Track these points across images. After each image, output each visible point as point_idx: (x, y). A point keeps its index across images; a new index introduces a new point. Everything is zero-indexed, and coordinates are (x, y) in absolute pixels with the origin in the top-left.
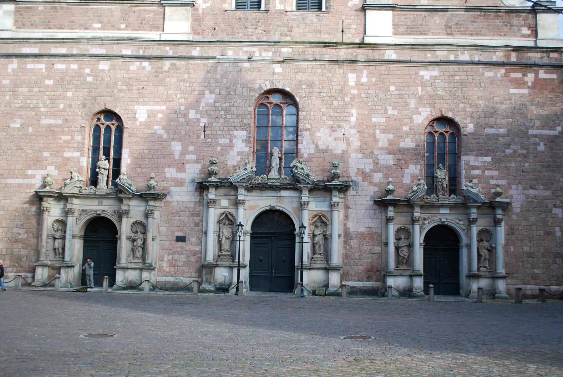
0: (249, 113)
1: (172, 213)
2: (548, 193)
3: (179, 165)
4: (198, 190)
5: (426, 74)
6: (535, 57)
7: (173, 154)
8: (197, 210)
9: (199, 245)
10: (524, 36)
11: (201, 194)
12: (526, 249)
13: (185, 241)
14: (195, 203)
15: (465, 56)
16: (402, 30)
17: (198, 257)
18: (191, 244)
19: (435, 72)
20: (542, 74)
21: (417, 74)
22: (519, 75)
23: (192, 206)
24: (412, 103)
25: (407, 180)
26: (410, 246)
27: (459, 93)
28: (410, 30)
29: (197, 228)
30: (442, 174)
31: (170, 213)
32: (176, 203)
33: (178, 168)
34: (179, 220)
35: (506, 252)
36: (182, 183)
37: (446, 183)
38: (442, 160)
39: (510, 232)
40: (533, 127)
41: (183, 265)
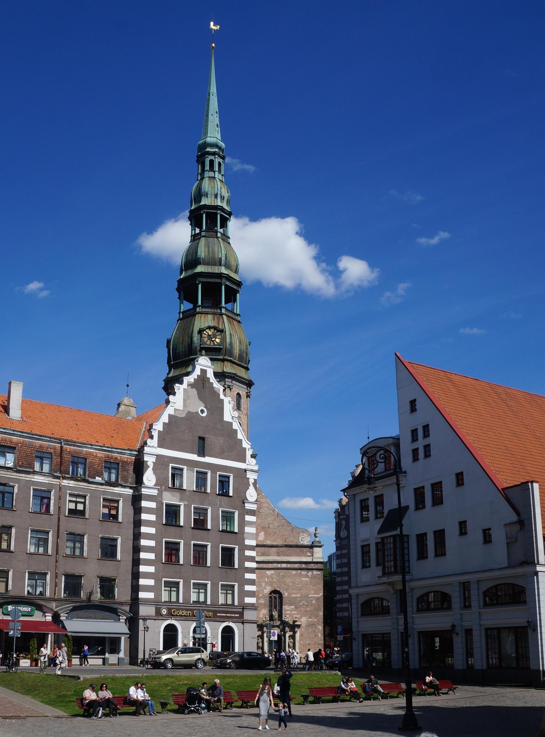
2: (316, 620)
5: (269, 573)
6: (312, 566)
10: (308, 556)
12: (307, 642)
15: (284, 566)
16: (259, 554)
19: (272, 572)
20: (315, 572)
21: (265, 573)
22: (306, 573)
24: (263, 585)
25: (261, 616)
26: (263, 642)
27: (282, 580)
28: (263, 554)
30: (275, 614)
35: (300, 643)
37: (277, 616)
38: (275, 607)
39: (301, 635)
40: (310, 594)
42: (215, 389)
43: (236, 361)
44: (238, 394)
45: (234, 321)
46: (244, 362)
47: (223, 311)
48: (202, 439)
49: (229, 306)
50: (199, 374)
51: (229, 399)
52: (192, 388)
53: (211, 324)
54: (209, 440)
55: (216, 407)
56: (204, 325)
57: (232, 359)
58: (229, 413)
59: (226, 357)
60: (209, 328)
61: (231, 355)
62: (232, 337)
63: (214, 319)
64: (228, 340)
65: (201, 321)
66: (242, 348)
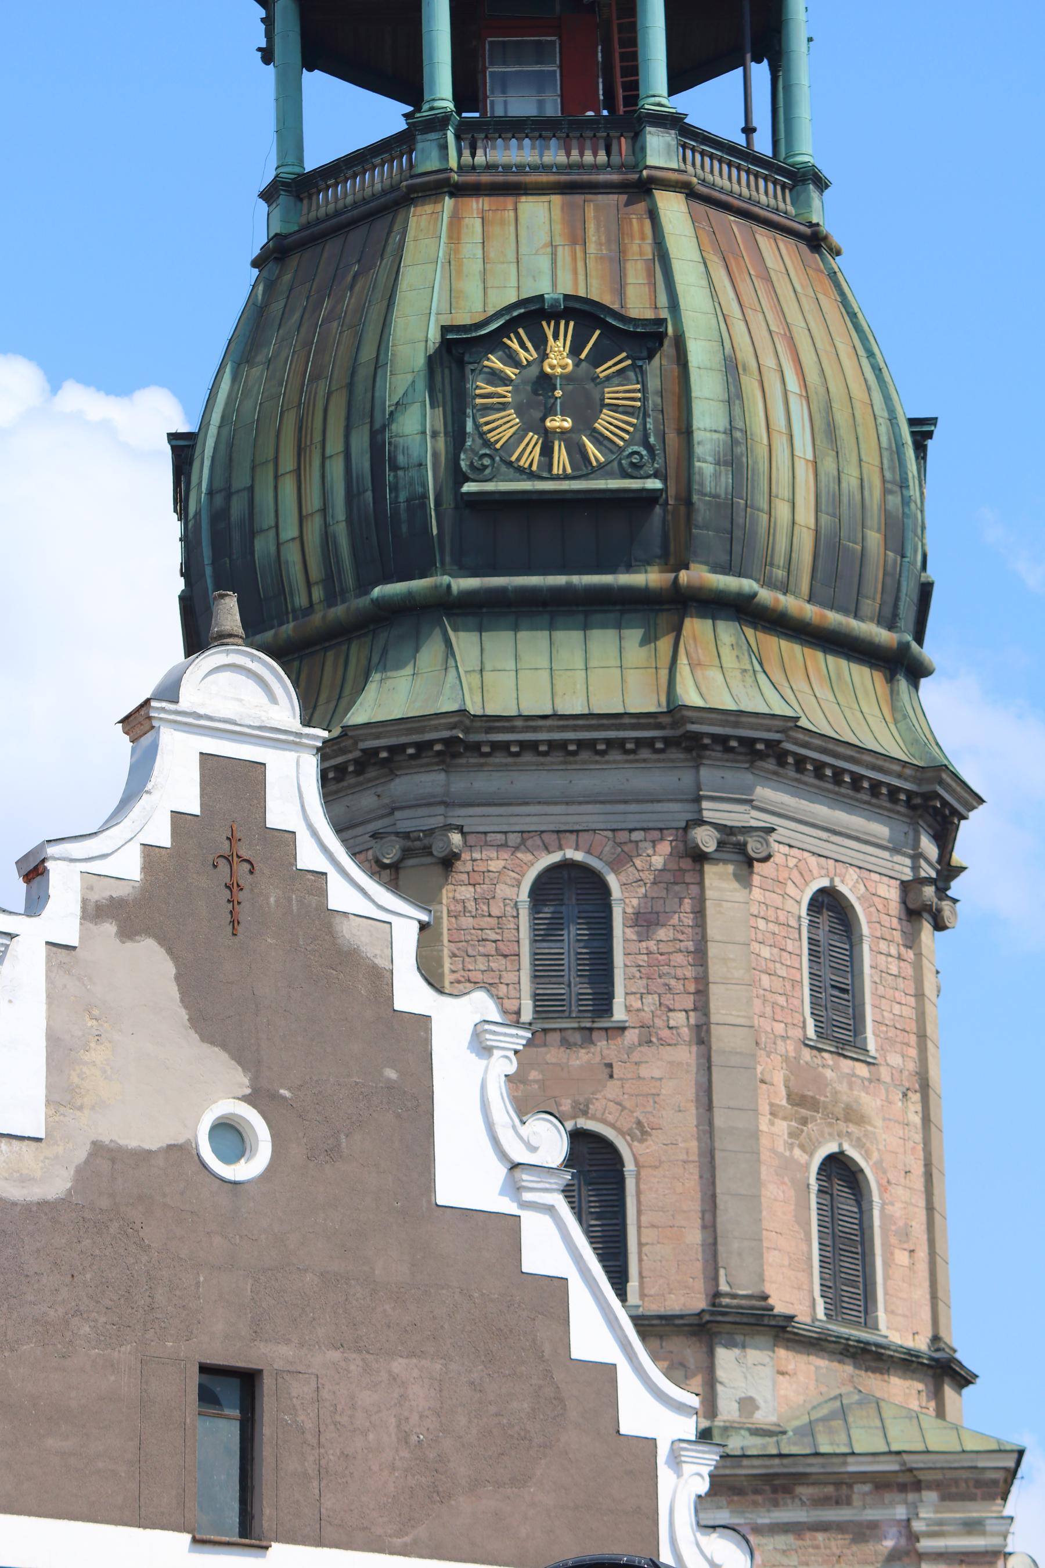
42: (350, 932)
43: (795, 605)
44: (829, 904)
45: (764, 239)
46: (870, 606)
47: (659, 150)
48: (233, 1388)
49: (717, 104)
50: (193, 806)
51: (480, 1005)
52: (127, 933)
53: (550, 278)
54: (300, 1389)
55: (359, 1095)
56: (479, 301)
57: (747, 585)
58: (483, 1140)
59: (699, 575)
60: (532, 316)
61: (738, 550)
62: (750, 385)
63: (577, 238)
64: (707, 417)
65: (453, 264)
66: (851, 481)
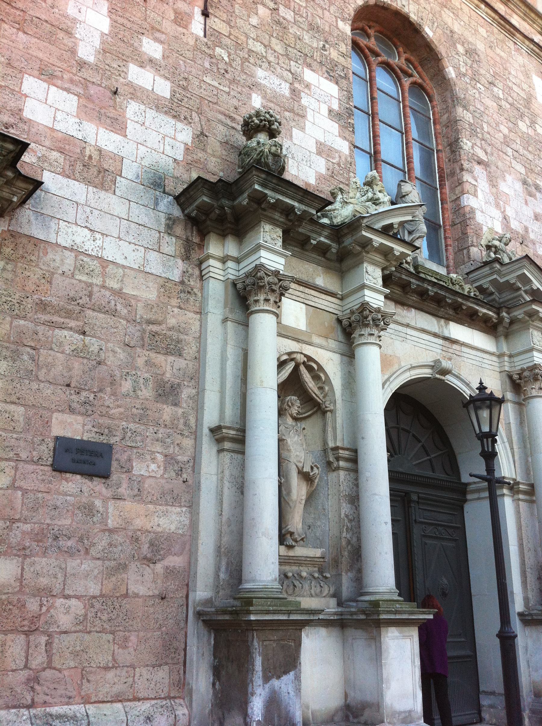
0: (341, 37)
1: (43, 306)
3: (93, 90)
4: (179, 230)
7: (69, 33)
8: (172, 322)
9: (176, 500)
11: (192, 254)
13: (105, 476)
14: (165, 284)
17: (170, 572)
18: (139, 495)
23: (151, 294)
29: (167, 412)
31: (29, 304)
32: (70, 259)
33: (89, 98)
34: (79, 353)
36: (102, 171)
41: (82, 624)
